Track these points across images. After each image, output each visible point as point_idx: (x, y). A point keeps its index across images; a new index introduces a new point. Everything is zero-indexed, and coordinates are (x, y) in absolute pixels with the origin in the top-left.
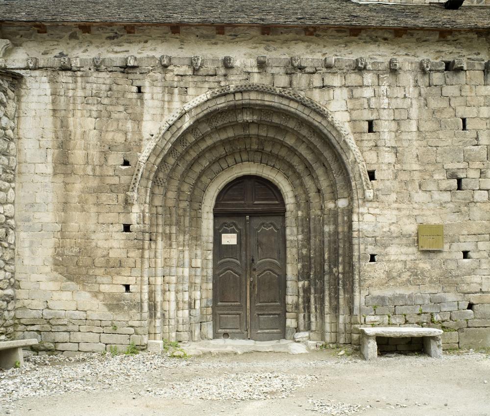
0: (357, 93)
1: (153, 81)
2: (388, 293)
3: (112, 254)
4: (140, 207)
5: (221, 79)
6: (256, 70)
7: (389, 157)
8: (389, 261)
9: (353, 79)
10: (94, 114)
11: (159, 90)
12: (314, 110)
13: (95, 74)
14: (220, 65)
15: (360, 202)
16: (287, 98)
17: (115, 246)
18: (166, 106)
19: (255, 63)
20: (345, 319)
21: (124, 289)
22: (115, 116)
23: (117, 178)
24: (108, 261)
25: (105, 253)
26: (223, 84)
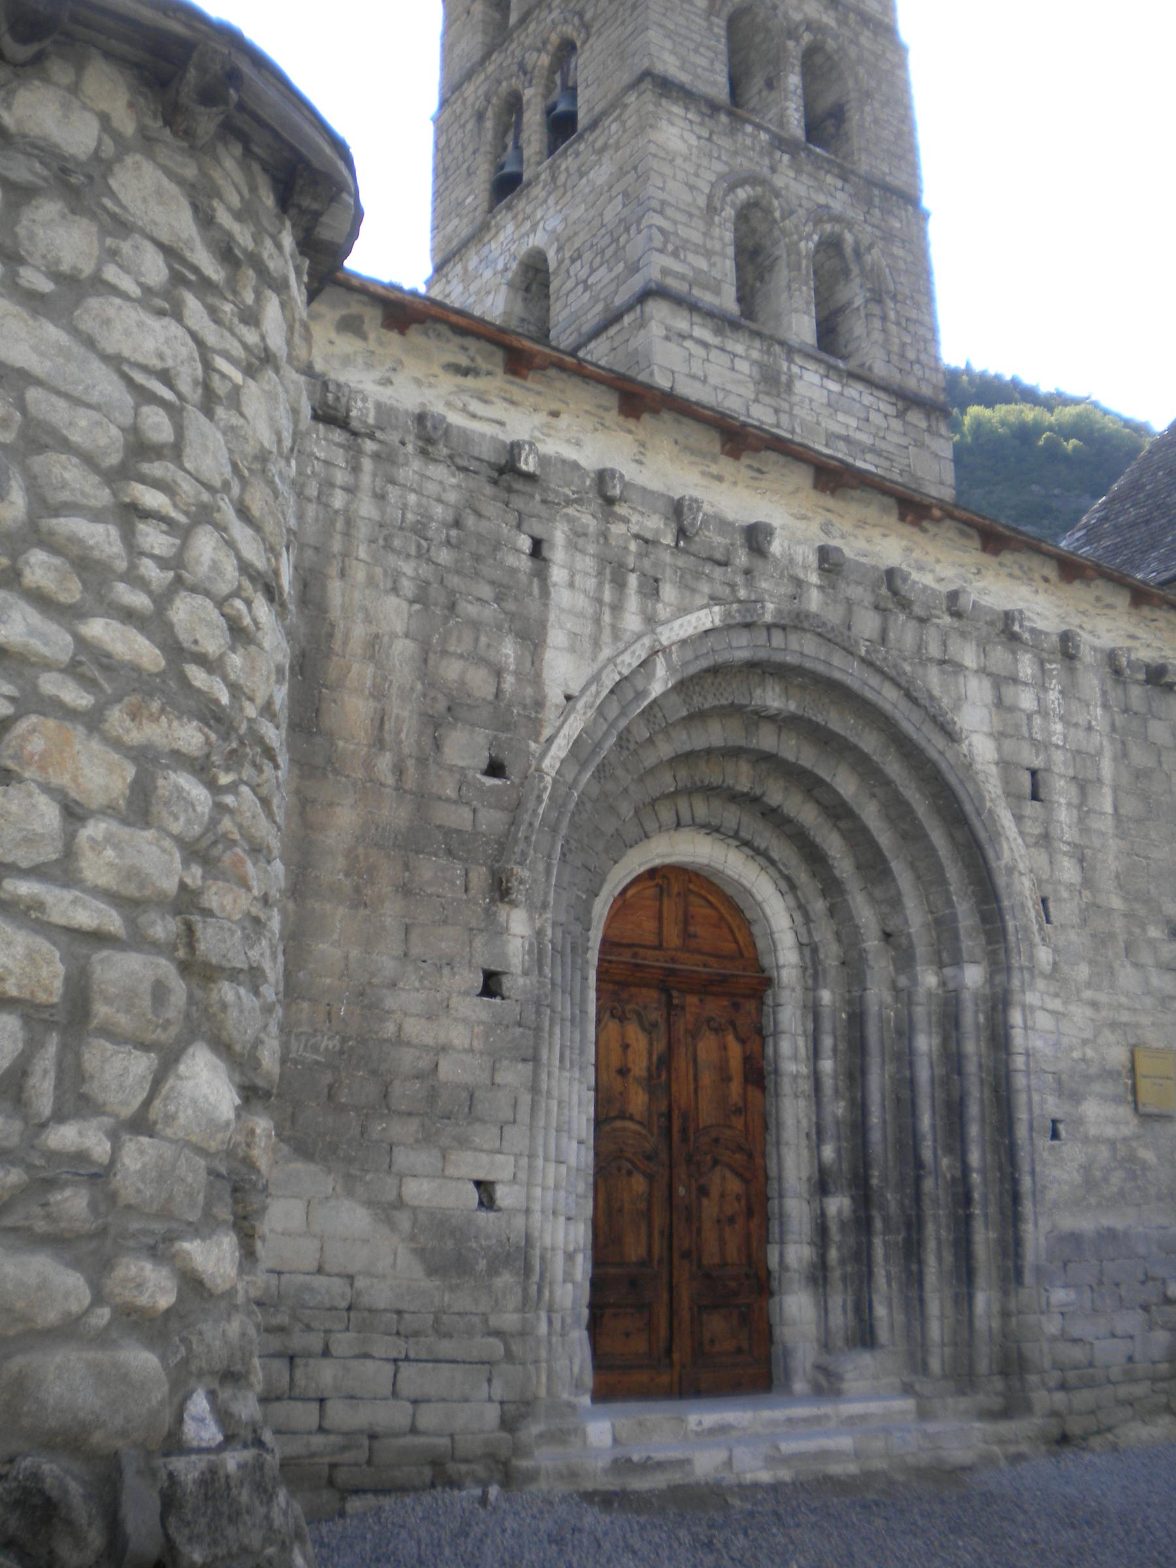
0: (1009, 692)
1: (577, 534)
2: (1087, 1224)
3: (448, 1070)
4: (531, 919)
5: (739, 579)
6: (814, 578)
7: (1069, 871)
8: (1086, 1140)
9: (999, 656)
10: (408, 587)
11: (587, 563)
12: (934, 719)
13: (416, 464)
14: (739, 540)
15: (1027, 975)
16: (880, 671)
17: (456, 1042)
18: (607, 618)
19: (813, 559)
20: (989, 1304)
21: (473, 1195)
22: (470, 609)
23: (466, 813)
24: (433, 1095)
25: (424, 1063)
26: (742, 593)
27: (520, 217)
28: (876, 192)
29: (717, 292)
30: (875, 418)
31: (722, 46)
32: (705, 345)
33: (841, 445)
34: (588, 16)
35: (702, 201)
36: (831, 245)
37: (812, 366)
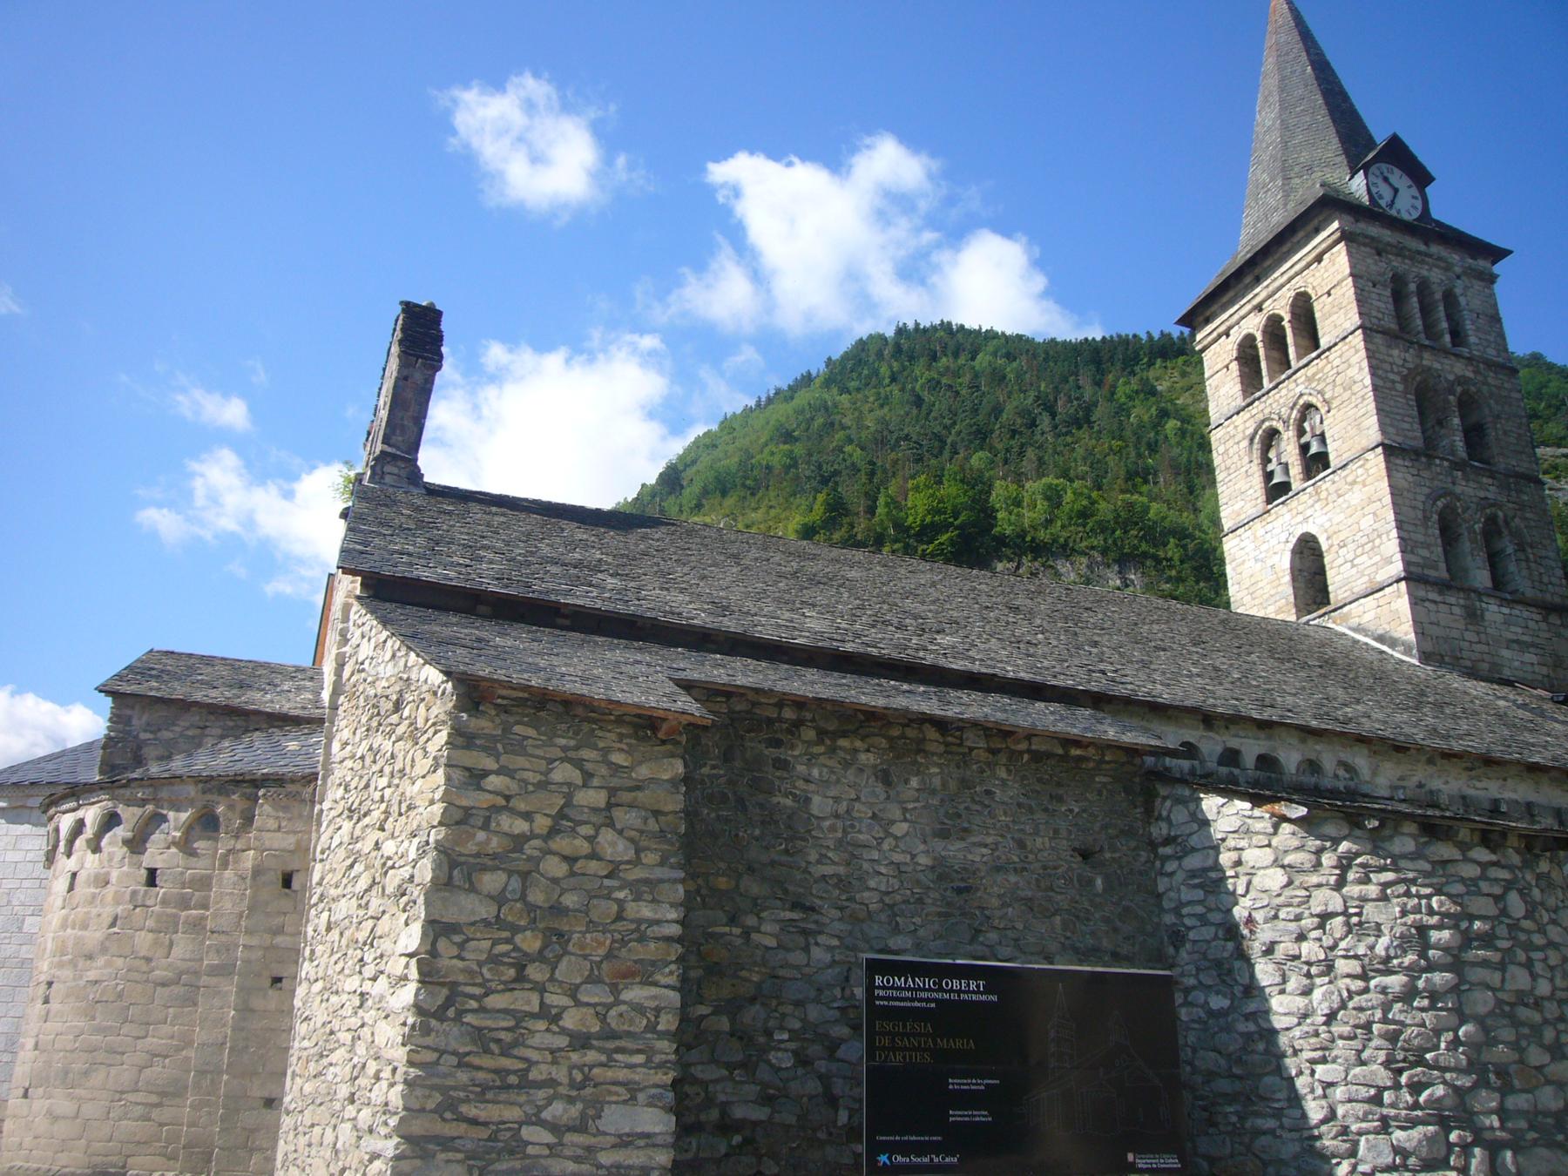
27: (1294, 512)
28: (1511, 480)
29: (1436, 568)
30: (1531, 624)
31: (1415, 413)
32: (1435, 602)
33: (1515, 646)
34: (1327, 396)
35: (1420, 514)
36: (1492, 520)
37: (1492, 601)
